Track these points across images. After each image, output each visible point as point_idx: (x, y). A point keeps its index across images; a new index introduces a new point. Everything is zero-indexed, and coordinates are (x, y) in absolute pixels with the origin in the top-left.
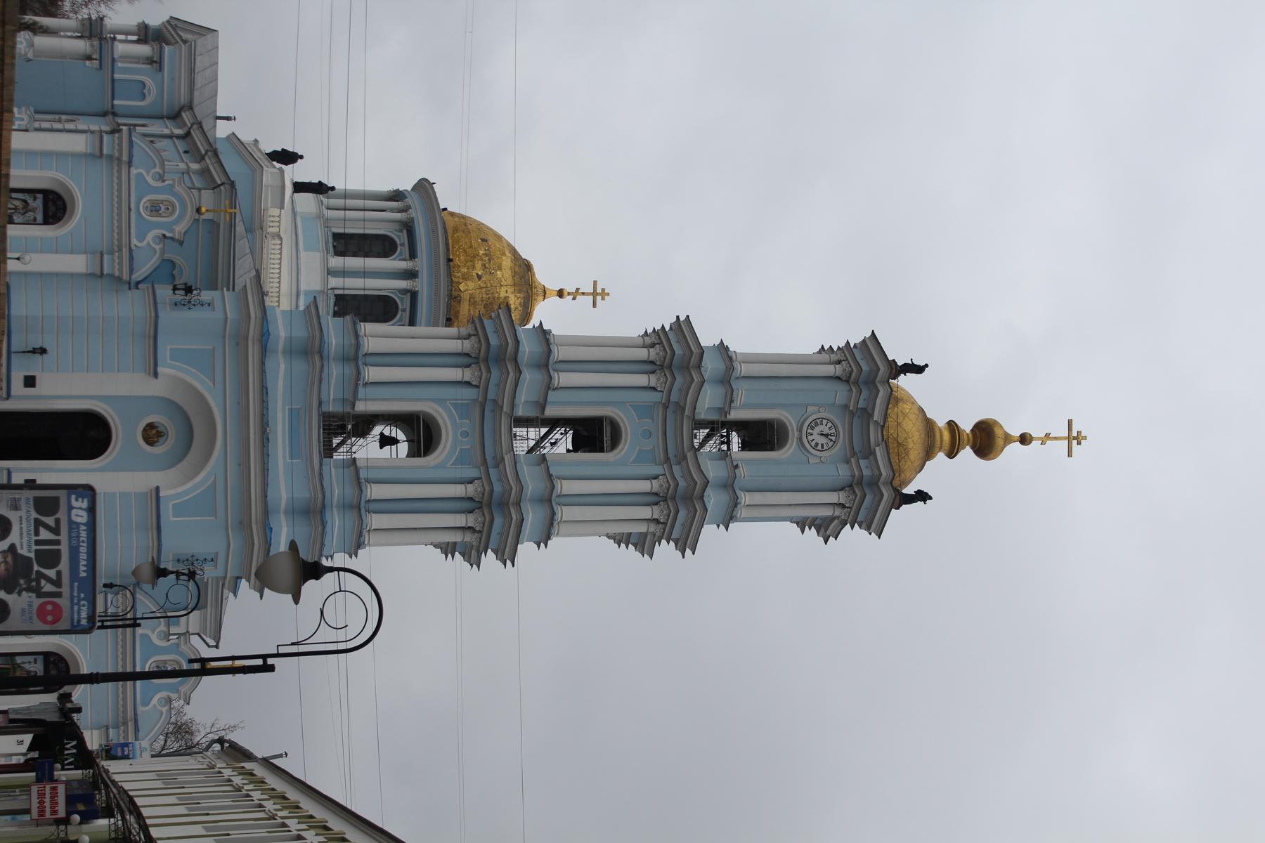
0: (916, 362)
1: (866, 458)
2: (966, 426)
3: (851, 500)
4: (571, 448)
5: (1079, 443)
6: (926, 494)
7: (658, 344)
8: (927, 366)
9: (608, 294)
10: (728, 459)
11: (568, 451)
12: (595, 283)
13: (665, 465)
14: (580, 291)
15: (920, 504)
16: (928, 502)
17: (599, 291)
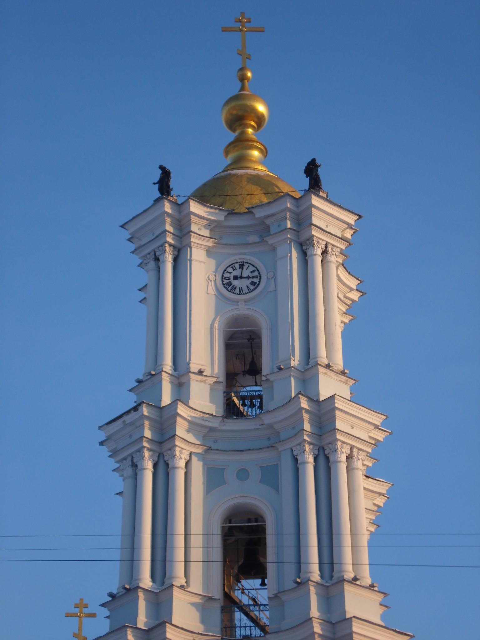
0: (157, 179)
2: (232, 136)
4: (259, 581)
5: (249, 21)
7: (132, 461)
8: (162, 168)
9: (81, 600)
10: (271, 378)
11: (263, 584)
12: (68, 615)
13: (280, 450)
14: (77, 631)
15: (321, 172)
16: (318, 162)
17: (77, 610)
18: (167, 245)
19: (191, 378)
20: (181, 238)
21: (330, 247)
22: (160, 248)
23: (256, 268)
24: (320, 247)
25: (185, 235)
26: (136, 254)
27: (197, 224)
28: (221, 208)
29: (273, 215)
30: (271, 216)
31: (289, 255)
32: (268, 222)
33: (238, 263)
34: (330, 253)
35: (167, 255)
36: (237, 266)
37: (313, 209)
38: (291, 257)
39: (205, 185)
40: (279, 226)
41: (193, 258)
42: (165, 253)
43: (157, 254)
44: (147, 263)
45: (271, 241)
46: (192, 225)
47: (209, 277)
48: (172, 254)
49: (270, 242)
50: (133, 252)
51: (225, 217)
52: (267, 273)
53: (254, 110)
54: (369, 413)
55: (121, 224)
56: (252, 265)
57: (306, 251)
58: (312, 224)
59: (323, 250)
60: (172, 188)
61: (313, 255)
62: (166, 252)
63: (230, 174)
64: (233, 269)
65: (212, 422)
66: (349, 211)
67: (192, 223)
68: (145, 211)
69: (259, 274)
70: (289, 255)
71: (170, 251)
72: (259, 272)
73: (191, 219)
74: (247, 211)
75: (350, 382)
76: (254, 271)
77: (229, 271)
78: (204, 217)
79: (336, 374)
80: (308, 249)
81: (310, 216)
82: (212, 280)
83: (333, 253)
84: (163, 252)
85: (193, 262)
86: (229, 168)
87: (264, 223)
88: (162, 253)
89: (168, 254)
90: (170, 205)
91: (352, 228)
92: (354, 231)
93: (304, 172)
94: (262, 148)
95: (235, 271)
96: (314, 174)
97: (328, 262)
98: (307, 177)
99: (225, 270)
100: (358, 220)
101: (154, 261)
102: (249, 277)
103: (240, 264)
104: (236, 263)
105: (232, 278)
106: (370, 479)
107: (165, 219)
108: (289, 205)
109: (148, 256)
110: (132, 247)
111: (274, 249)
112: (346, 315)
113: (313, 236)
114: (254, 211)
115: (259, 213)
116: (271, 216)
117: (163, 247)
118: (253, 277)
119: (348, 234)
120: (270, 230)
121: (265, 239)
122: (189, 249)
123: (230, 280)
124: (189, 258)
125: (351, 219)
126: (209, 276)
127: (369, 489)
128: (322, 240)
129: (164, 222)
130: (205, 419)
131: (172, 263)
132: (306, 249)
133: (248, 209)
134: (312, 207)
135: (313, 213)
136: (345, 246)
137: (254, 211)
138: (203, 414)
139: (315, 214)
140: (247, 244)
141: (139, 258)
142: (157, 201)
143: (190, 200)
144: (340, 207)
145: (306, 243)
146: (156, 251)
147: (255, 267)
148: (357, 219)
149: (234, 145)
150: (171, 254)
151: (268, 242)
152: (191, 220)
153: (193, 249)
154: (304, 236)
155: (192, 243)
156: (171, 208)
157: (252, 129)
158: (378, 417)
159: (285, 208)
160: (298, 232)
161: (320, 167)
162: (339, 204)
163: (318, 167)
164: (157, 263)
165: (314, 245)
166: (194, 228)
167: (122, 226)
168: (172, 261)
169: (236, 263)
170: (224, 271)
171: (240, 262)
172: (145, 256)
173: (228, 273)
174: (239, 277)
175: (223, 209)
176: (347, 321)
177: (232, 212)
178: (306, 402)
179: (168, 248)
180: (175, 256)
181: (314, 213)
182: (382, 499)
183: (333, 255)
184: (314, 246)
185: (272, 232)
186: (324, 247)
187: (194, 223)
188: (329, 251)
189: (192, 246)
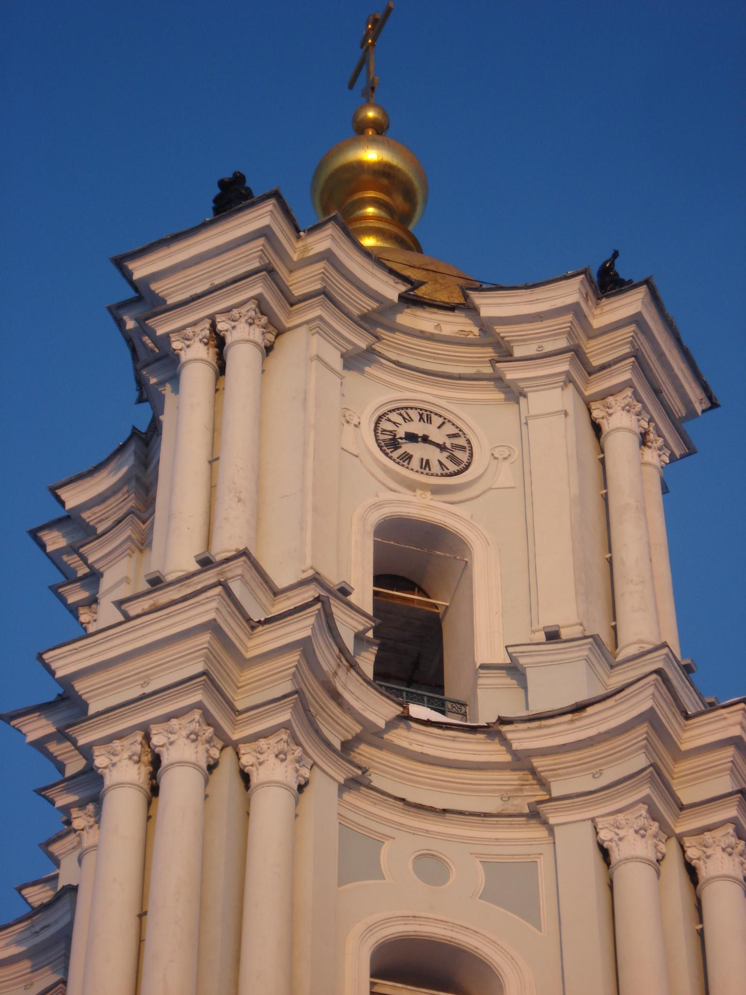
19: (56, 854)
21: (223, 319)
37: (154, 287)
54: (169, 616)
65: (56, 922)
75: (231, 570)
79: (182, 586)
90: (58, 531)
106: (590, 710)
112: (613, 368)
113: (167, 336)
127: (600, 734)
128: (195, 324)
130: (37, 928)
135: (160, 295)
138: (29, 921)
143: (57, 491)
158: (201, 604)
176: (627, 376)
178: (44, 722)
181: (162, 291)
182: (725, 718)
187: (100, 522)
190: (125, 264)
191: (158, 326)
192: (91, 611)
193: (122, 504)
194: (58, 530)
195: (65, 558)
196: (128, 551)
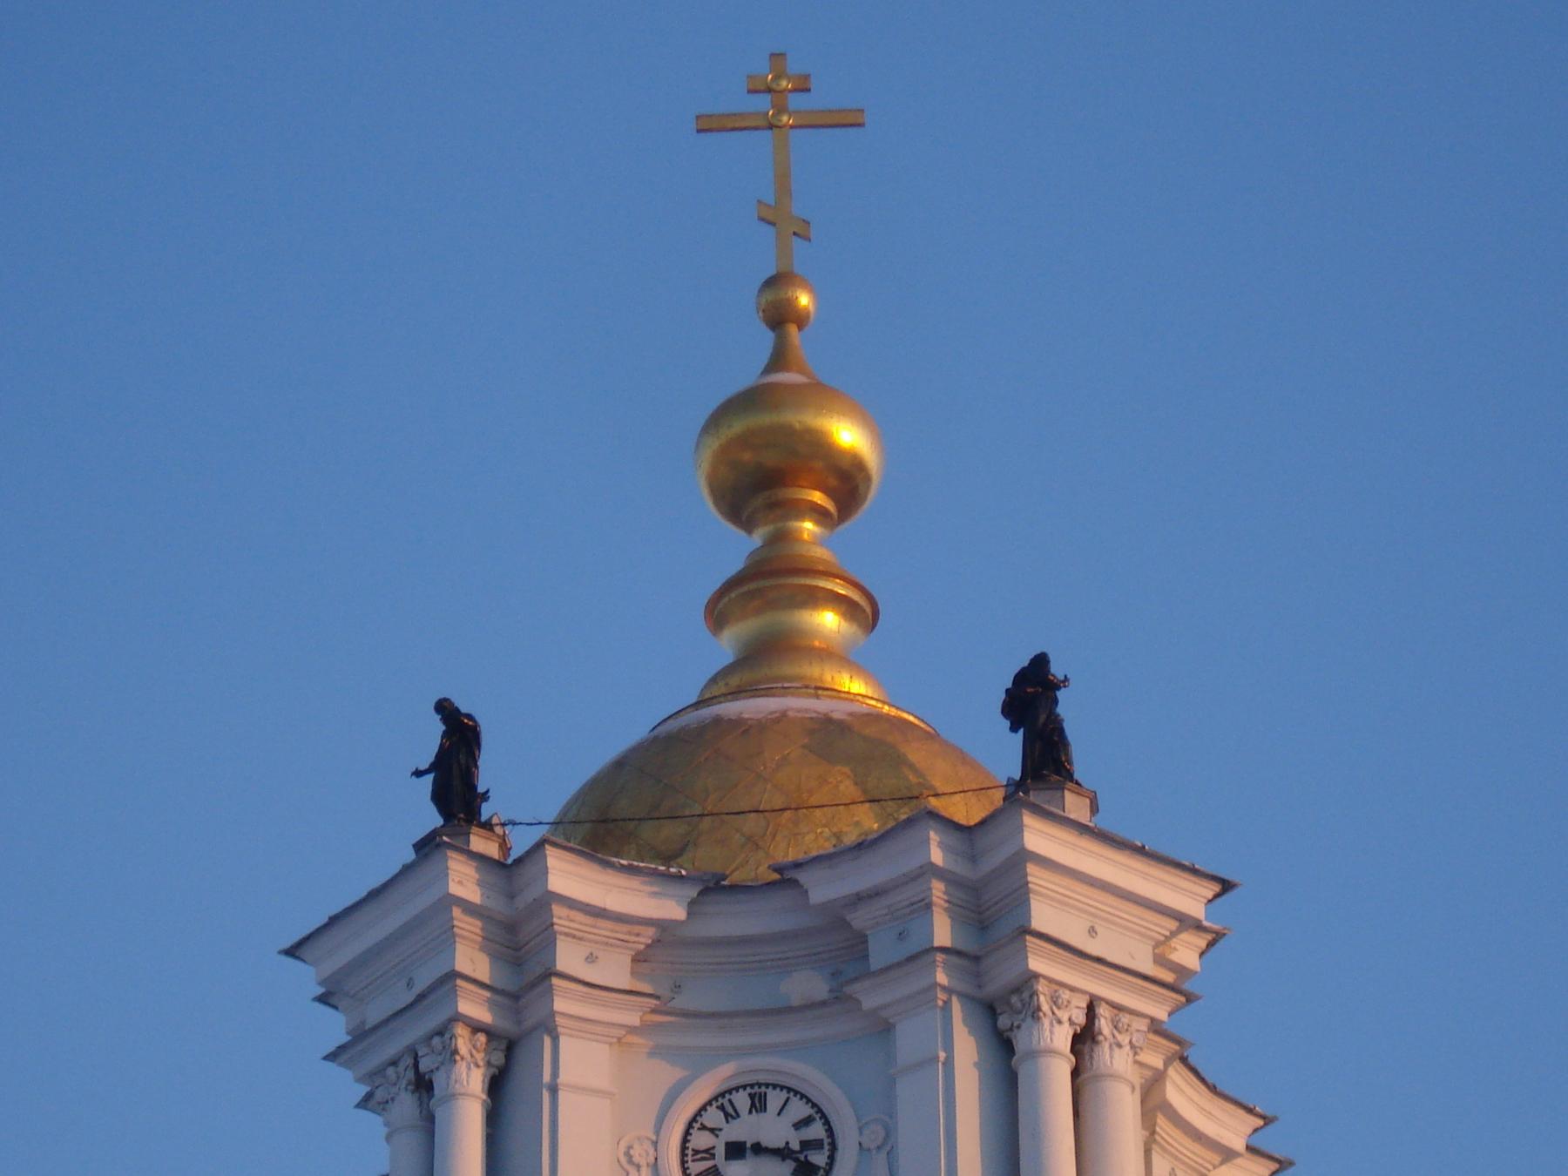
1: (858, 945)
3: (1055, 1001)
6: (1022, 678)
15: (1068, 706)
16: (1057, 669)
18: (461, 1031)
20: (515, 997)
21: (1107, 1015)
22: (436, 1041)
23: (816, 1109)
24: (1065, 1018)
25: (533, 985)
26: (347, 1065)
27: (581, 939)
28: (672, 870)
29: (876, 893)
30: (870, 897)
31: (942, 1055)
32: (859, 919)
33: (744, 1087)
34: (1106, 1039)
35: (461, 1067)
36: (742, 1100)
38: (949, 1063)
39: (619, 764)
40: (901, 936)
41: (562, 1079)
42: (455, 1061)
43: (424, 1065)
44: (387, 1102)
45: (872, 997)
46: (558, 942)
47: (632, 1152)
48: (481, 1063)
49: (868, 1003)
50: (332, 1057)
51: (692, 905)
52: (861, 1129)
53: (821, 447)
55: (287, 944)
56: (803, 1096)
57: (1009, 1033)
58: (1027, 931)
59: (1076, 1030)
60: (488, 791)
61: (1034, 1054)
62: (458, 1058)
63: (718, 720)
64: (727, 1115)
66: (1179, 866)
67: (558, 936)
68: (374, 895)
69: (830, 1131)
70: (942, 1055)
71: (474, 1052)
72: (827, 1123)
73: (555, 920)
74: (776, 876)
76: (806, 1122)
77: (709, 1125)
78: (605, 910)
80: (1019, 1027)
81: (1021, 896)
82: (643, 1163)
83: (1119, 1037)
84: (448, 1056)
85: (562, 1095)
86: (716, 691)
87: (846, 925)
88: (442, 1063)
89: (464, 1064)
91: (1198, 927)
92: (1209, 937)
93: (1003, 712)
94: (855, 596)
95: (735, 1121)
96: (1042, 718)
97: (1098, 1077)
98: (1014, 729)
99: (694, 1120)
100: (1219, 900)
101: (413, 1092)
102: (789, 1149)
103: (753, 1091)
104: (737, 1089)
105: (720, 1151)
107: (453, 927)
108: (937, 856)
109: (391, 1071)
110: (334, 1027)
111: (887, 1029)
113: (1036, 976)
114: (802, 877)
115: (823, 888)
116: (870, 897)
117: (447, 1036)
118: (806, 1145)
119: (1187, 952)
120: (867, 949)
121: (848, 990)
122: (547, 1041)
123: (714, 1159)
124: (547, 1078)
125: (1190, 898)
126: (630, 1147)
128: (1073, 989)
129: (448, 937)
131: (484, 1101)
132: (1011, 1029)
133: (779, 869)
134: (1026, 861)
135: (1030, 885)
136: (1169, 1009)
137: (802, 877)
139: (1041, 889)
140: (784, 1011)
141: (359, 1080)
142: (427, 846)
143: (547, 846)
144: (1140, 851)
145: (1008, 1003)
146: (420, 1054)
147: (814, 1105)
148: (1217, 896)
149: (752, 586)
150: (478, 1066)
151: (858, 1002)
152: (555, 927)
153: (563, 1040)
154: (1000, 978)
155: (559, 1020)
156: (480, 883)
157: (817, 522)
159: (921, 867)
160: (976, 959)
161: (1065, 687)
162: (1140, 844)
163: (1059, 688)
164: (425, 1095)
165: (1041, 1014)
166: (568, 957)
167: (292, 952)
168: (484, 1097)
169: (737, 1089)
170: (690, 1126)
171: (752, 1086)
172: (380, 1071)
173: (707, 1133)
174: (748, 1145)
175: (682, 876)
177: (717, 883)
179: (463, 1041)
180: (493, 1070)
183: (1120, 1046)
184: (1039, 1018)
185: (876, 962)
186: (1080, 1018)
187: (567, 935)
188: (1101, 1033)
189: (559, 1029)
190: (1024, 811)
191: (1035, 954)
192: (470, 1040)
193: (619, 942)
194: (478, 870)
195: (456, 912)
196: (615, 1040)
